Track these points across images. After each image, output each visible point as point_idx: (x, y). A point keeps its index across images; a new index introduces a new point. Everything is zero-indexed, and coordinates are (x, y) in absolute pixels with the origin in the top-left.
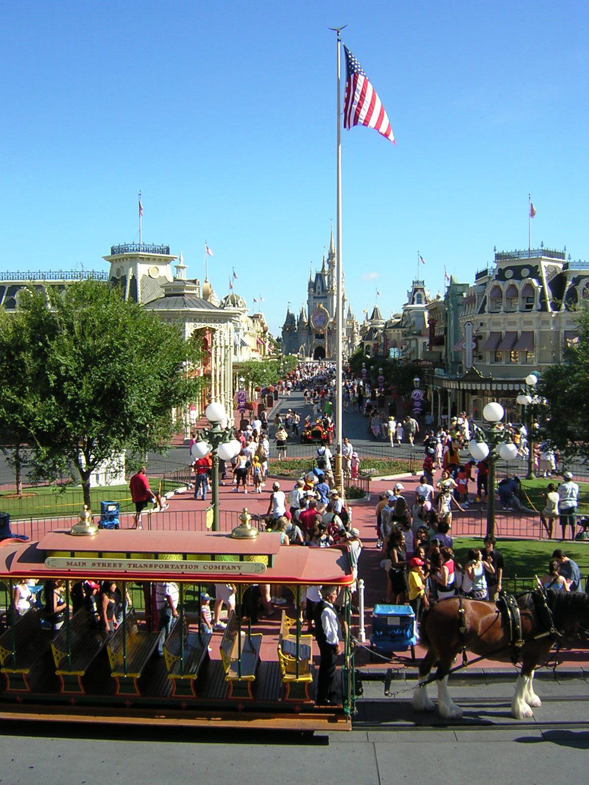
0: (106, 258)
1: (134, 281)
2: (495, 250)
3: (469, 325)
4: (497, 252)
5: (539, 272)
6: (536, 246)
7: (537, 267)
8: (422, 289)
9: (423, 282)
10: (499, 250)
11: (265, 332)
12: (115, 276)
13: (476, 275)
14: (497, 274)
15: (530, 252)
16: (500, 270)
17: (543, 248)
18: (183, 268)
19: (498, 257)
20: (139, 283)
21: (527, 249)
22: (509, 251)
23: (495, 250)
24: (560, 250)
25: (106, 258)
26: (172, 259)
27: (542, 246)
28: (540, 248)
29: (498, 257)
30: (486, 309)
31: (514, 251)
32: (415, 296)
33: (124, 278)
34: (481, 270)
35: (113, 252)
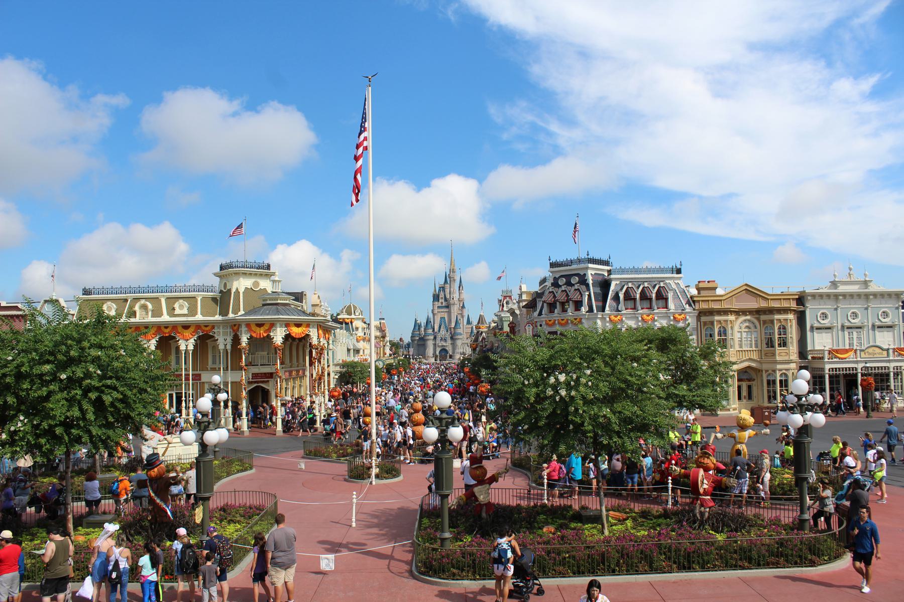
0: (215, 275)
1: (237, 292)
2: (550, 260)
3: (529, 326)
4: (551, 261)
6: (583, 256)
7: (585, 275)
8: (510, 297)
10: (553, 260)
11: (384, 337)
12: (223, 289)
15: (580, 261)
17: (589, 257)
18: (279, 281)
19: (553, 265)
20: (241, 295)
21: (576, 258)
23: (550, 260)
24: (605, 258)
25: (215, 275)
26: (273, 274)
28: (586, 257)
29: (553, 265)
30: (543, 313)
32: (505, 302)
33: (230, 290)
34: (543, 277)
35: (222, 268)
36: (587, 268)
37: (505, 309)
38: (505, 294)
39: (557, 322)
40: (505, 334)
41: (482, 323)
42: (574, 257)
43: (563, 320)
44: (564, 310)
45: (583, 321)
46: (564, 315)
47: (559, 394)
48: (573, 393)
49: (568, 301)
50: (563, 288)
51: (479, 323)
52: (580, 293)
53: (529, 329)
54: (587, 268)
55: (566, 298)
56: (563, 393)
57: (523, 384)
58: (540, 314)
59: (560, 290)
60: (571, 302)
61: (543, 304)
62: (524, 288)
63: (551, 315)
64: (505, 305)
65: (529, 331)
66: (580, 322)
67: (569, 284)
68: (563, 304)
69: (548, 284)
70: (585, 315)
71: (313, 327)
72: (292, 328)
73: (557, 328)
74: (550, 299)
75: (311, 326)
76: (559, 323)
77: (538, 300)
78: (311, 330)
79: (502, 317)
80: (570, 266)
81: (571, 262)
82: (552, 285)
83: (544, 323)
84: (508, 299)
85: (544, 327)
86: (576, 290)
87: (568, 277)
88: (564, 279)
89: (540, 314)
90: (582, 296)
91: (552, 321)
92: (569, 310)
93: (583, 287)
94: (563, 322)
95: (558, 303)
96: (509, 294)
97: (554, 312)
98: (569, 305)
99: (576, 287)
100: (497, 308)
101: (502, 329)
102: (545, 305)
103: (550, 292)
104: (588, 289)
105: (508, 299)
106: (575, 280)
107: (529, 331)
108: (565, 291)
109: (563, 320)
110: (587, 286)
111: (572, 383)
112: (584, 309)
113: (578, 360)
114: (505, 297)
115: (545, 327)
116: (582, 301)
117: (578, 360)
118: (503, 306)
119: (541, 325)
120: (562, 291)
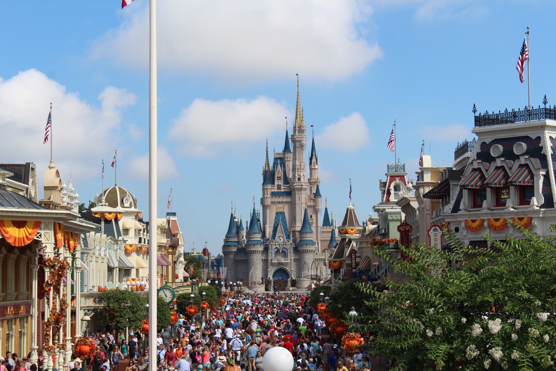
2: (475, 111)
4: (477, 114)
5: (542, 148)
6: (536, 104)
7: (539, 139)
8: (402, 178)
9: (404, 166)
10: (481, 111)
11: (174, 246)
13: (456, 153)
14: (480, 151)
15: (529, 113)
16: (483, 145)
17: (547, 106)
19: (480, 121)
21: (522, 109)
22: (497, 112)
23: (475, 111)
27: (545, 103)
28: (542, 106)
29: (480, 121)
30: (462, 207)
31: (503, 111)
36: (544, 127)
37: (392, 198)
38: (393, 172)
39: (486, 224)
40: (392, 245)
41: (351, 224)
42: (519, 105)
43: (497, 220)
44: (500, 203)
45: (535, 222)
46: (498, 211)
47: (491, 357)
48: (516, 355)
49: (506, 187)
50: (499, 162)
51: (344, 223)
52: (530, 172)
53: (435, 235)
54: (544, 127)
55: (503, 181)
56: (497, 353)
57: (424, 335)
58: (456, 209)
59: (493, 166)
60: (512, 188)
61: (461, 191)
62: (428, 163)
63: (475, 212)
64: (392, 192)
65: (436, 240)
66: (529, 225)
67: (509, 155)
68: (497, 191)
69: (471, 154)
70: (538, 212)
71: (47, 228)
72: (8, 229)
73: (486, 235)
74: (475, 182)
75: (43, 226)
76: (491, 226)
77: (452, 183)
78: (42, 232)
79: (387, 214)
80: (512, 122)
81: (514, 116)
82: (479, 156)
83: (463, 225)
84: (398, 181)
85: (463, 233)
86: (521, 166)
87: (508, 143)
88: (501, 147)
89: (456, 209)
90: (532, 177)
91: (478, 223)
92: (509, 203)
93: (535, 162)
94: (498, 224)
95: (488, 190)
96: (400, 173)
97: (481, 206)
98: (508, 194)
99: (522, 161)
100: (377, 197)
101: (386, 234)
102: (465, 192)
103: (474, 170)
104: (545, 166)
105: (398, 181)
106: (520, 148)
107: (436, 240)
108: (502, 167)
109: (497, 220)
110: (543, 159)
111: (514, 336)
112: (536, 202)
113: (525, 294)
114: (393, 178)
115: (465, 232)
116: (532, 187)
117: (525, 294)
118: (389, 194)
119: (457, 230)
120: (497, 168)
